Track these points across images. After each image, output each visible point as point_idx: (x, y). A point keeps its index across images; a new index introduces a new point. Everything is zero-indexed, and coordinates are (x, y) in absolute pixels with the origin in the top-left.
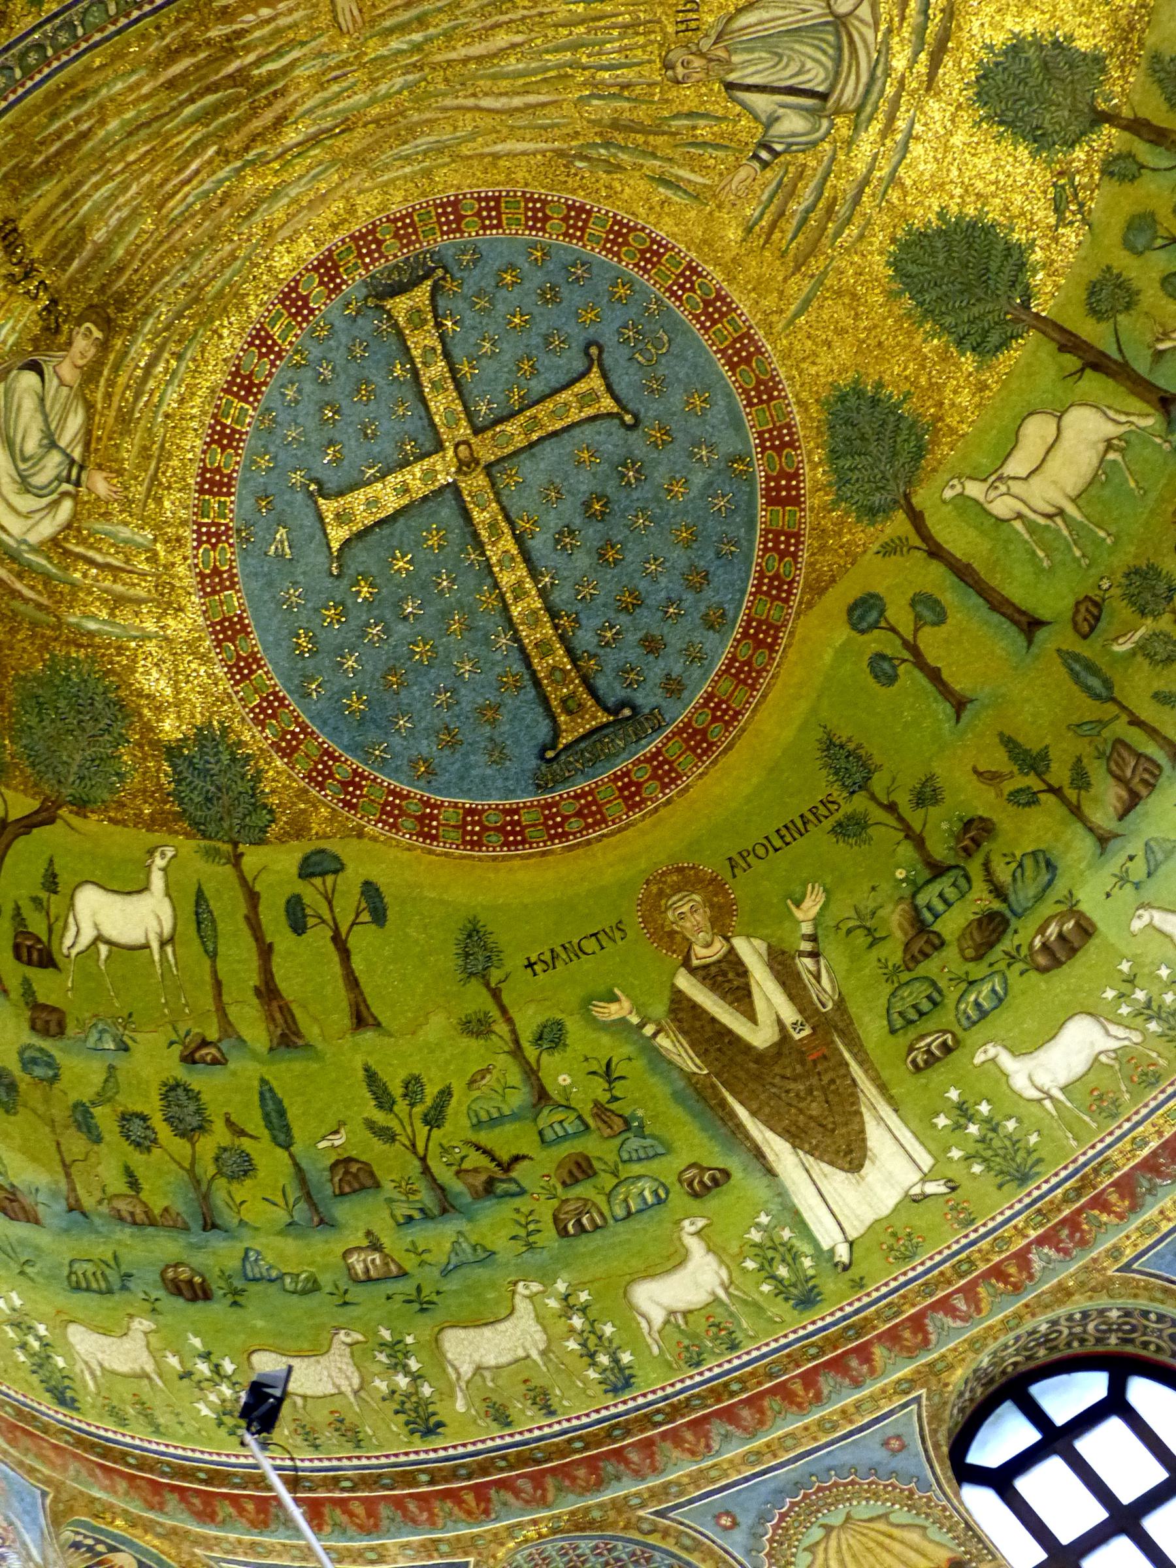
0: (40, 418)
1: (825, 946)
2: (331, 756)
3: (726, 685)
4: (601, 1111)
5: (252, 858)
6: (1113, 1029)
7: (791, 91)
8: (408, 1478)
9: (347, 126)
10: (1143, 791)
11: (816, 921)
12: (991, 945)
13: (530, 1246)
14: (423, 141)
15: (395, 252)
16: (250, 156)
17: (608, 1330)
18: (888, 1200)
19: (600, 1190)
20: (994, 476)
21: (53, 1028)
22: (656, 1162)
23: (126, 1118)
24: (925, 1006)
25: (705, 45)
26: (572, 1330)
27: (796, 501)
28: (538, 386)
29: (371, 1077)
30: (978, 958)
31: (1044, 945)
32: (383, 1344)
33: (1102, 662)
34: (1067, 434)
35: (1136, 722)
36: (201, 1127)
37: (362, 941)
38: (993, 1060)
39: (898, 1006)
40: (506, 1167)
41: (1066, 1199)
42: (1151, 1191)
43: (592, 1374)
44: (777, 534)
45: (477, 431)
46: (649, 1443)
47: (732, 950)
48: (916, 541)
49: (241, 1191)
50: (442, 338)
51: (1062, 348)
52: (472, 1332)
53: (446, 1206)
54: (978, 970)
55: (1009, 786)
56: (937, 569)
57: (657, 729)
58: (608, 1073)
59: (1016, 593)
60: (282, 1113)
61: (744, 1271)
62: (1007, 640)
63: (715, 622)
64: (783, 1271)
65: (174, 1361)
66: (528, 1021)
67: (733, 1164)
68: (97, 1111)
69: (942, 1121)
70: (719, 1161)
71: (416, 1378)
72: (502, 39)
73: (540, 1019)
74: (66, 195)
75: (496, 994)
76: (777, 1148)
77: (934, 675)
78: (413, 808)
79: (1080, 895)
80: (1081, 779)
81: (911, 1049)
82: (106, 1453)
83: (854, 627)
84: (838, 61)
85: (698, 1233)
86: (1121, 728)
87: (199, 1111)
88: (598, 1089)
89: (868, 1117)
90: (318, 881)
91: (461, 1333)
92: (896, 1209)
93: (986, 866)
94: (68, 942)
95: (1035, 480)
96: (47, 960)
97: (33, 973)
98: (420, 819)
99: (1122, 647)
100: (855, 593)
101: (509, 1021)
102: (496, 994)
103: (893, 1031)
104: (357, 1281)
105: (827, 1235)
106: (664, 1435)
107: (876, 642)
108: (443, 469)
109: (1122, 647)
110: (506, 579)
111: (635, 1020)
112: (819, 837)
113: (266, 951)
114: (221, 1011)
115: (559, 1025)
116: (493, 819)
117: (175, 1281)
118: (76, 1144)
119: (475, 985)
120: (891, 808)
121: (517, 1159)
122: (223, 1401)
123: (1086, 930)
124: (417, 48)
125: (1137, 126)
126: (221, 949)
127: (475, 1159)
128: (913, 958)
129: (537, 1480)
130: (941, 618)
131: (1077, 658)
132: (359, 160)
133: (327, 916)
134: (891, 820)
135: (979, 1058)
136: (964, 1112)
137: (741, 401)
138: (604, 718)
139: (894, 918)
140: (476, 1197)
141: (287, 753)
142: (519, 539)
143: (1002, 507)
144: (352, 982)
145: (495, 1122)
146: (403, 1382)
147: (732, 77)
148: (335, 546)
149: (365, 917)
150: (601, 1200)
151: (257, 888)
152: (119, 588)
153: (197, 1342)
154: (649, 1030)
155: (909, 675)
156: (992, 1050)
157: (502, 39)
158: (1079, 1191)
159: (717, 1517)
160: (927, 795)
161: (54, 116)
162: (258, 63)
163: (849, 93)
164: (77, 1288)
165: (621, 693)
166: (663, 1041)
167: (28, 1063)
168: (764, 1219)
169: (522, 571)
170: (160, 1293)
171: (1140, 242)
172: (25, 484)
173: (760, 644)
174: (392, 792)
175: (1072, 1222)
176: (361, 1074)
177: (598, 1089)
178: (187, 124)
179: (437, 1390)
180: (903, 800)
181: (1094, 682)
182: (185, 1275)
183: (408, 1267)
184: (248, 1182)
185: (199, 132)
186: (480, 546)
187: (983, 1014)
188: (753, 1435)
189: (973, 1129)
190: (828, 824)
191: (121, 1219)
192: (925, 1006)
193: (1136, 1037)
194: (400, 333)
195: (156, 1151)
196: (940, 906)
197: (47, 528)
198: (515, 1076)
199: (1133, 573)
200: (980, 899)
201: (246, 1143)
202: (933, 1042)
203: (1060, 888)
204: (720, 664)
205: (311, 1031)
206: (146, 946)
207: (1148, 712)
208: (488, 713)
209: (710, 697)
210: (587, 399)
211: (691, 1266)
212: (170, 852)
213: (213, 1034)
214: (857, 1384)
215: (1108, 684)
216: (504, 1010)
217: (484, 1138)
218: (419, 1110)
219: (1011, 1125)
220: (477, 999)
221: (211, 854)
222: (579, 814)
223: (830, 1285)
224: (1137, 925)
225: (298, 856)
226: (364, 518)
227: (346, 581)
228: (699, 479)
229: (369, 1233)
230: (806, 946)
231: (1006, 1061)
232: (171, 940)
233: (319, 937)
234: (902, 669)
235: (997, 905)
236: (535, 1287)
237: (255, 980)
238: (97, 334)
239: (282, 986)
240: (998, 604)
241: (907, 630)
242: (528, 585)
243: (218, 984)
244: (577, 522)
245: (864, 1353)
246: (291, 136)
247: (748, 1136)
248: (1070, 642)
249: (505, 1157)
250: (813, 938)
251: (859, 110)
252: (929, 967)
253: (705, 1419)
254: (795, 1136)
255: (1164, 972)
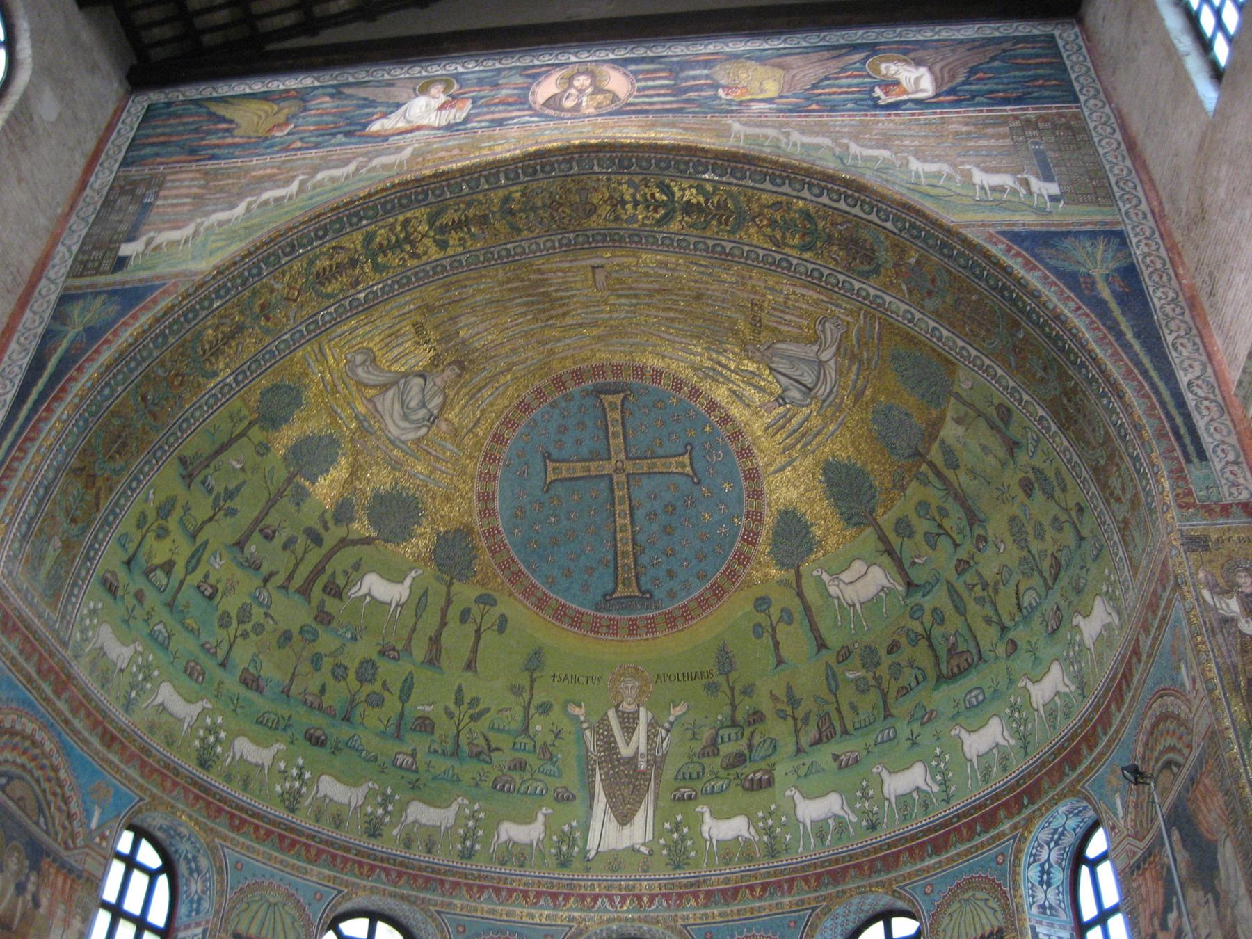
0: (420, 396)
1: (675, 730)
2: (513, 560)
3: (694, 604)
4: (545, 747)
5: (457, 587)
6: (752, 831)
7: (797, 381)
8: (347, 849)
9: (595, 324)
10: (824, 739)
11: (677, 718)
12: (733, 766)
13: (477, 785)
14: (631, 341)
15: (610, 378)
16: (550, 322)
17: (480, 833)
18: (626, 843)
19: (521, 778)
20: (835, 576)
21: (326, 621)
22: (550, 779)
23: (337, 665)
24: (694, 776)
25: (762, 349)
26: (466, 825)
27: (754, 544)
28: (660, 452)
29: (459, 690)
30: (726, 769)
31: (752, 779)
32: (384, 794)
33: (840, 678)
34: (870, 575)
35: (838, 710)
36: (370, 681)
37: (486, 637)
38: (702, 814)
39: (684, 770)
40: (490, 750)
41: (686, 886)
42: (716, 903)
43: (459, 847)
44: (741, 554)
45: (627, 458)
46: (455, 885)
47: (638, 712)
48: (794, 585)
49: (369, 711)
50: (623, 418)
51: (879, 538)
52: (425, 807)
53: (456, 753)
54: (723, 773)
55: (779, 706)
56: (797, 600)
57: (657, 608)
58: (557, 735)
59: (824, 627)
60: (410, 689)
61: (551, 839)
62: (809, 646)
63: (702, 577)
64: (564, 848)
65: (282, 765)
66: (540, 697)
67: (581, 796)
68: (325, 659)
69: (667, 825)
70: (574, 792)
71: (387, 813)
72: (672, 314)
73: (545, 699)
74: (451, 319)
75: (532, 681)
76: (601, 799)
77: (776, 644)
78: (539, 594)
79: (777, 767)
80: (806, 720)
81: (677, 790)
82: (206, 790)
83: (755, 607)
84: (818, 378)
85: (545, 815)
86: (831, 709)
87: (374, 674)
88: (550, 739)
89: (642, 807)
90: (482, 606)
91: (421, 805)
92: (624, 850)
93: (752, 734)
94: (352, 591)
95: (850, 587)
96: (338, 594)
97: (327, 598)
98: (539, 600)
99: (850, 675)
100: (762, 594)
101: (532, 695)
102: (532, 681)
103: (676, 778)
104: (394, 763)
105: (592, 844)
106: (466, 884)
107: (761, 618)
108: (608, 468)
109: (850, 675)
110: (619, 522)
111: (582, 718)
112: (699, 684)
113: (443, 624)
114: (410, 639)
115: (551, 705)
116: (571, 613)
117: (311, 736)
118: (305, 668)
119: (526, 674)
120: (732, 689)
121: (498, 749)
122: (291, 787)
123: (770, 783)
124: (635, 305)
125: (931, 465)
126: (424, 615)
127: (481, 742)
128: (703, 754)
129: (400, 874)
130: (790, 623)
131: (832, 669)
132: (599, 338)
133: (478, 621)
134: (729, 693)
135: (699, 809)
136: (677, 827)
137: (745, 494)
138: (637, 593)
139: (706, 734)
140: (471, 756)
141: (493, 553)
142: (631, 508)
143: (833, 590)
144: (475, 651)
145: (499, 730)
146: (380, 811)
147: (773, 365)
148: (549, 480)
149: (495, 628)
150: (518, 782)
151: (454, 598)
152: (439, 466)
153: (300, 761)
154: (585, 725)
155: (767, 639)
156: (705, 808)
157: (672, 314)
158: (692, 885)
159: (459, 925)
160: (748, 691)
161: (448, 291)
162: (556, 291)
163: (822, 391)
164: (261, 723)
165: (649, 586)
166: (588, 733)
167: (301, 631)
168: (574, 823)
169: (628, 521)
170: (300, 737)
171: (922, 513)
172: (405, 417)
173: (715, 595)
174: (534, 585)
175: (680, 896)
176: (456, 687)
177: (550, 739)
178: (517, 305)
179: (391, 822)
180: (738, 688)
181: (833, 683)
182: (319, 733)
183: (420, 769)
184: (376, 709)
185: (524, 309)
186: (613, 504)
187: (712, 792)
188: (500, 904)
189: (675, 836)
190: (705, 681)
191: (305, 702)
192: (694, 776)
193: (757, 838)
194: (604, 409)
195: (343, 683)
196: (726, 739)
197: (412, 436)
198: (519, 716)
199: (868, 647)
200: (742, 746)
201: (386, 694)
202: (687, 792)
203: (770, 761)
204: (696, 594)
205: (444, 663)
206: (390, 604)
207: (845, 708)
208: (590, 570)
209: (685, 606)
210: (683, 465)
211: (533, 826)
212: (420, 572)
213: (400, 647)
214: (555, 907)
215: (837, 687)
216: (532, 688)
217: (491, 735)
218: (471, 711)
219: (689, 843)
220: (524, 680)
221: (437, 578)
222: (608, 627)
223: (577, 864)
224: (788, 793)
225: (477, 593)
226: (564, 474)
227: (547, 496)
228: (717, 517)
229: (414, 750)
230: (667, 725)
231: (707, 816)
232: (402, 606)
233: (470, 628)
234: (766, 634)
235: (746, 752)
236: (466, 802)
237: (432, 633)
238: (457, 370)
239: (443, 640)
240: (814, 629)
241: (775, 619)
242: (629, 527)
243: (414, 630)
244: (659, 511)
245: (567, 897)
246: (569, 321)
247: (593, 788)
248: (833, 662)
249: (493, 745)
250: (672, 724)
251: (824, 401)
252: (706, 761)
253: (487, 887)
254: (610, 797)
255: (784, 819)
